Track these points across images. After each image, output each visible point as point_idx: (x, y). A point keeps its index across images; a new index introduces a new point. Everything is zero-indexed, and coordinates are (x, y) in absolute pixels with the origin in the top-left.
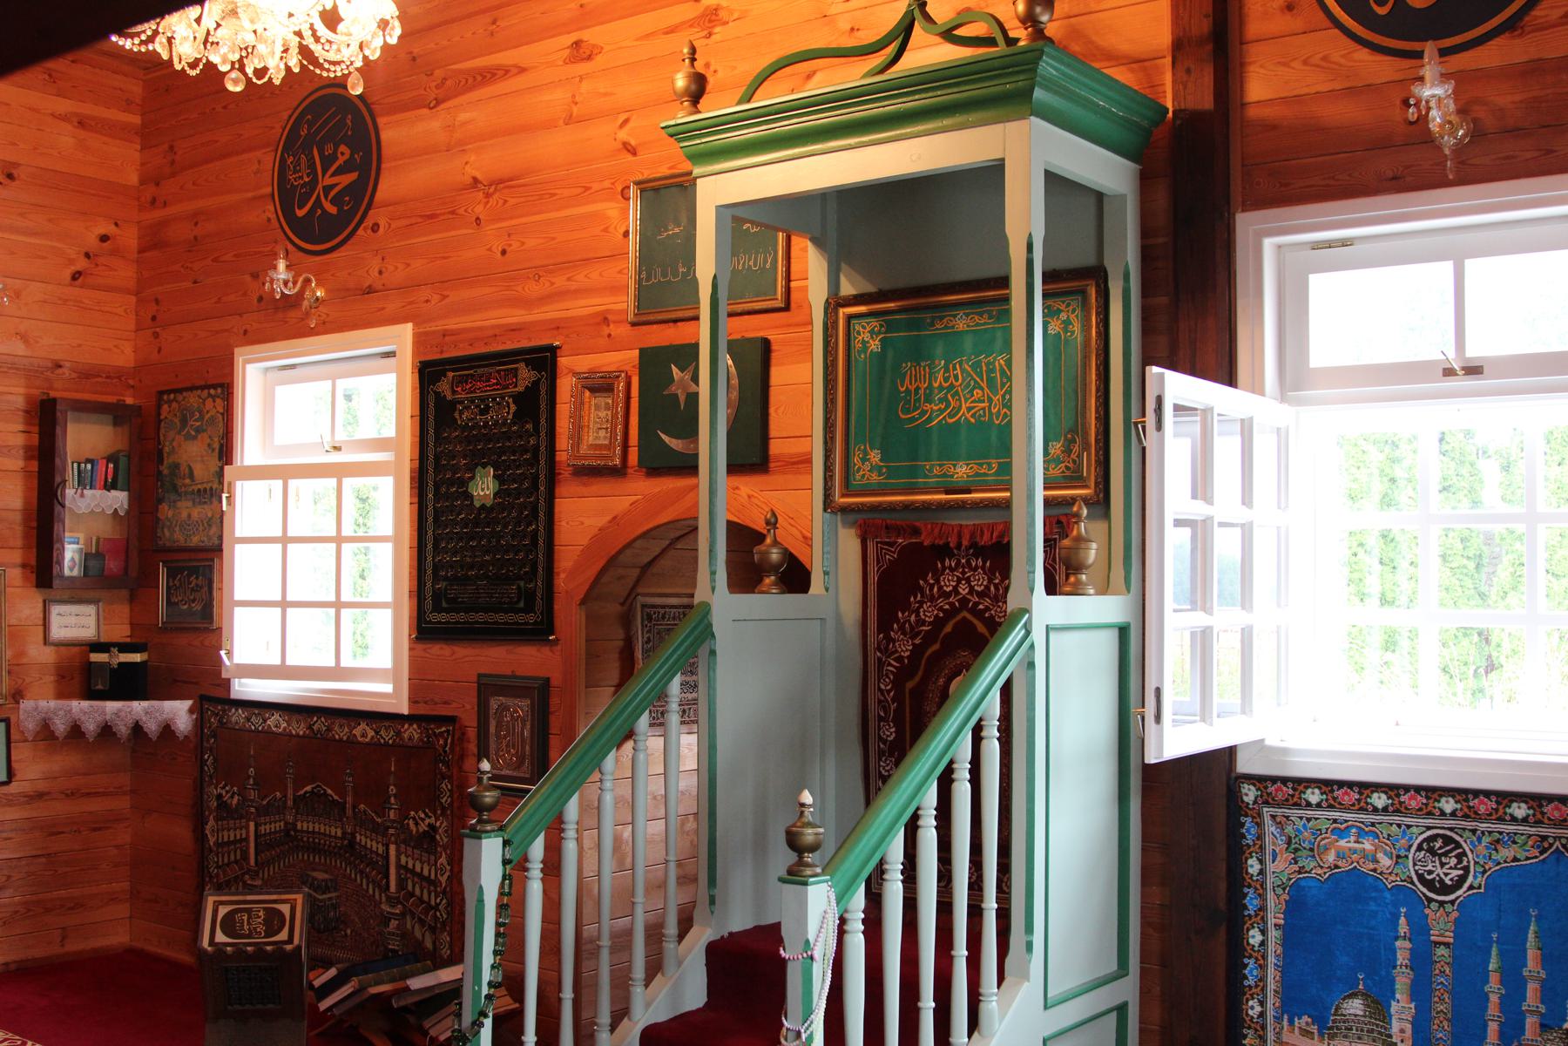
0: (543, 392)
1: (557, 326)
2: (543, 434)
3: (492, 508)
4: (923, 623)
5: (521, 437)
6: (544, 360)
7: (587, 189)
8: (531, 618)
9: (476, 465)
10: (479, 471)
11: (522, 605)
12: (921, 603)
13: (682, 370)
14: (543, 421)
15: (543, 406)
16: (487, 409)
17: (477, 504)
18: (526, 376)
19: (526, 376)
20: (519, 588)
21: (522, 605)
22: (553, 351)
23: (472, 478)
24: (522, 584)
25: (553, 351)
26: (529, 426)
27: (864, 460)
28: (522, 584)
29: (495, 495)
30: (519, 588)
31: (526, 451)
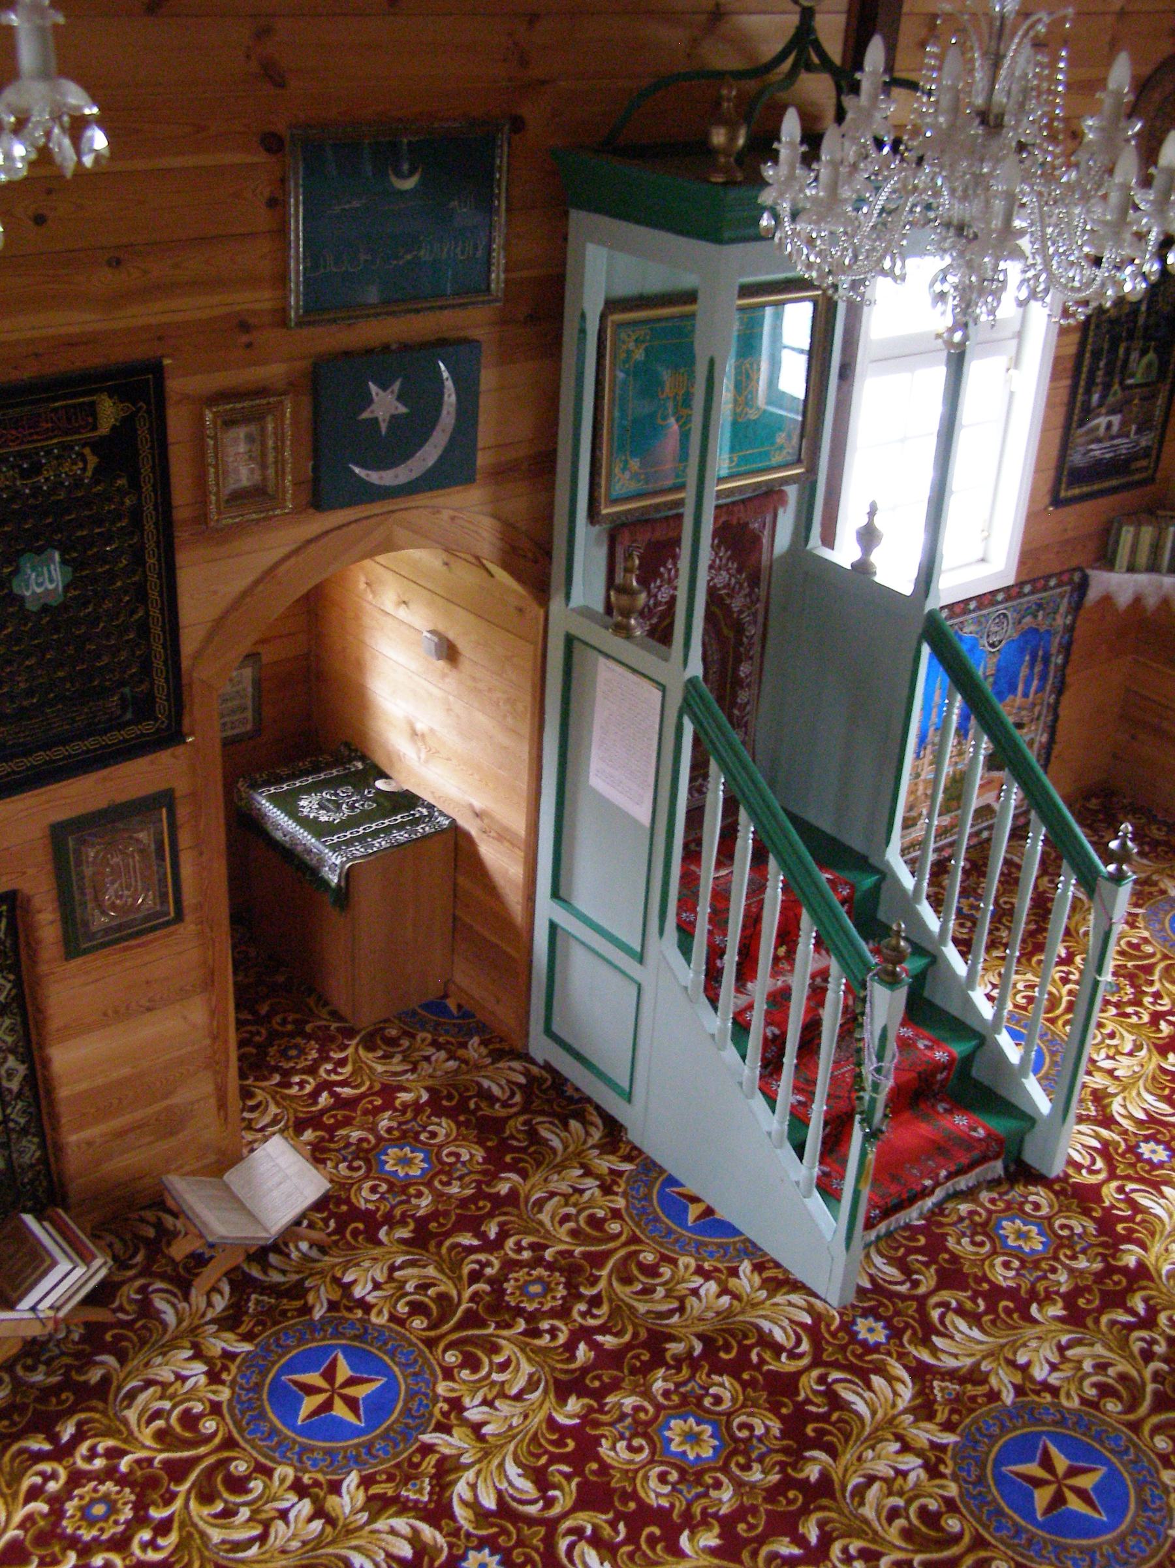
0: (143, 432)
2: (147, 489)
3: (64, 607)
4: (660, 603)
5: (110, 500)
6: (141, 383)
8: (148, 727)
9: (20, 553)
10: (27, 563)
12: (659, 587)
14: (146, 471)
16: (36, 469)
17: (32, 607)
18: (109, 412)
21: (129, 716)
22: (156, 369)
23: (16, 572)
27: (624, 469)
28: (127, 690)
29: (67, 588)
30: (123, 698)
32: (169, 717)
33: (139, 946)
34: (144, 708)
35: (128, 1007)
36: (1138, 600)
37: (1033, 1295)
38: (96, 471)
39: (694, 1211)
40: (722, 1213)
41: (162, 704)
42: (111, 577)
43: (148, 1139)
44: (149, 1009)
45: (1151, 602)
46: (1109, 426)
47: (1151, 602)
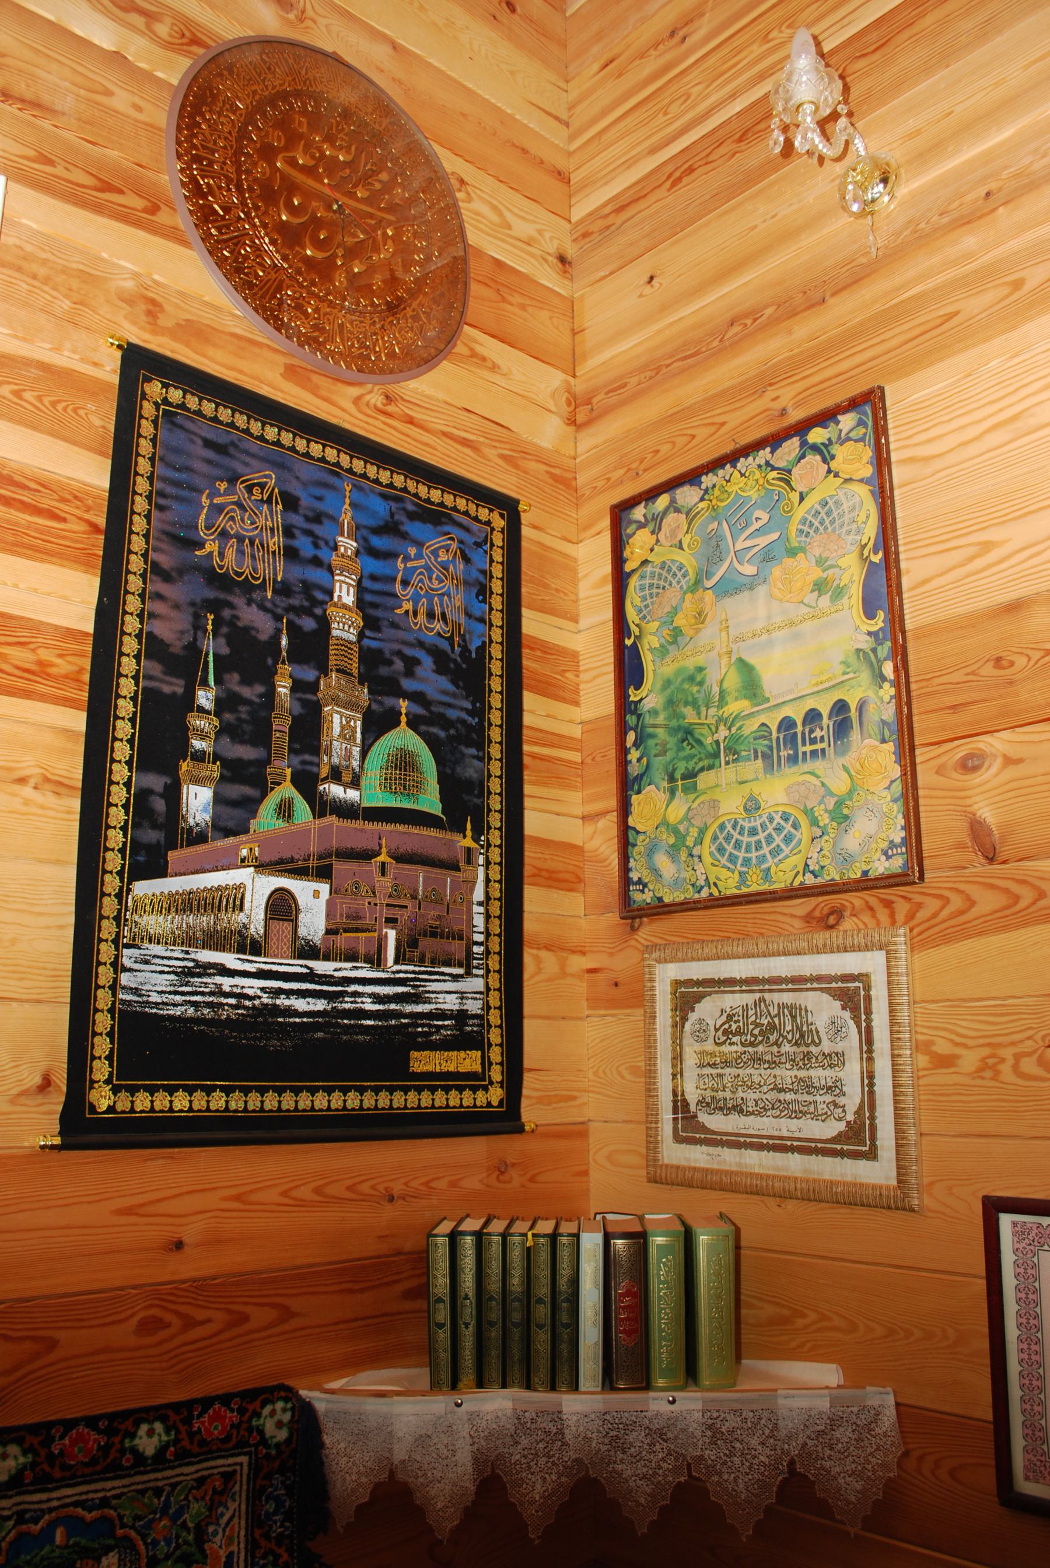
36: (492, 1481)
45: (537, 1486)
46: (282, 907)
47: (537, 1486)
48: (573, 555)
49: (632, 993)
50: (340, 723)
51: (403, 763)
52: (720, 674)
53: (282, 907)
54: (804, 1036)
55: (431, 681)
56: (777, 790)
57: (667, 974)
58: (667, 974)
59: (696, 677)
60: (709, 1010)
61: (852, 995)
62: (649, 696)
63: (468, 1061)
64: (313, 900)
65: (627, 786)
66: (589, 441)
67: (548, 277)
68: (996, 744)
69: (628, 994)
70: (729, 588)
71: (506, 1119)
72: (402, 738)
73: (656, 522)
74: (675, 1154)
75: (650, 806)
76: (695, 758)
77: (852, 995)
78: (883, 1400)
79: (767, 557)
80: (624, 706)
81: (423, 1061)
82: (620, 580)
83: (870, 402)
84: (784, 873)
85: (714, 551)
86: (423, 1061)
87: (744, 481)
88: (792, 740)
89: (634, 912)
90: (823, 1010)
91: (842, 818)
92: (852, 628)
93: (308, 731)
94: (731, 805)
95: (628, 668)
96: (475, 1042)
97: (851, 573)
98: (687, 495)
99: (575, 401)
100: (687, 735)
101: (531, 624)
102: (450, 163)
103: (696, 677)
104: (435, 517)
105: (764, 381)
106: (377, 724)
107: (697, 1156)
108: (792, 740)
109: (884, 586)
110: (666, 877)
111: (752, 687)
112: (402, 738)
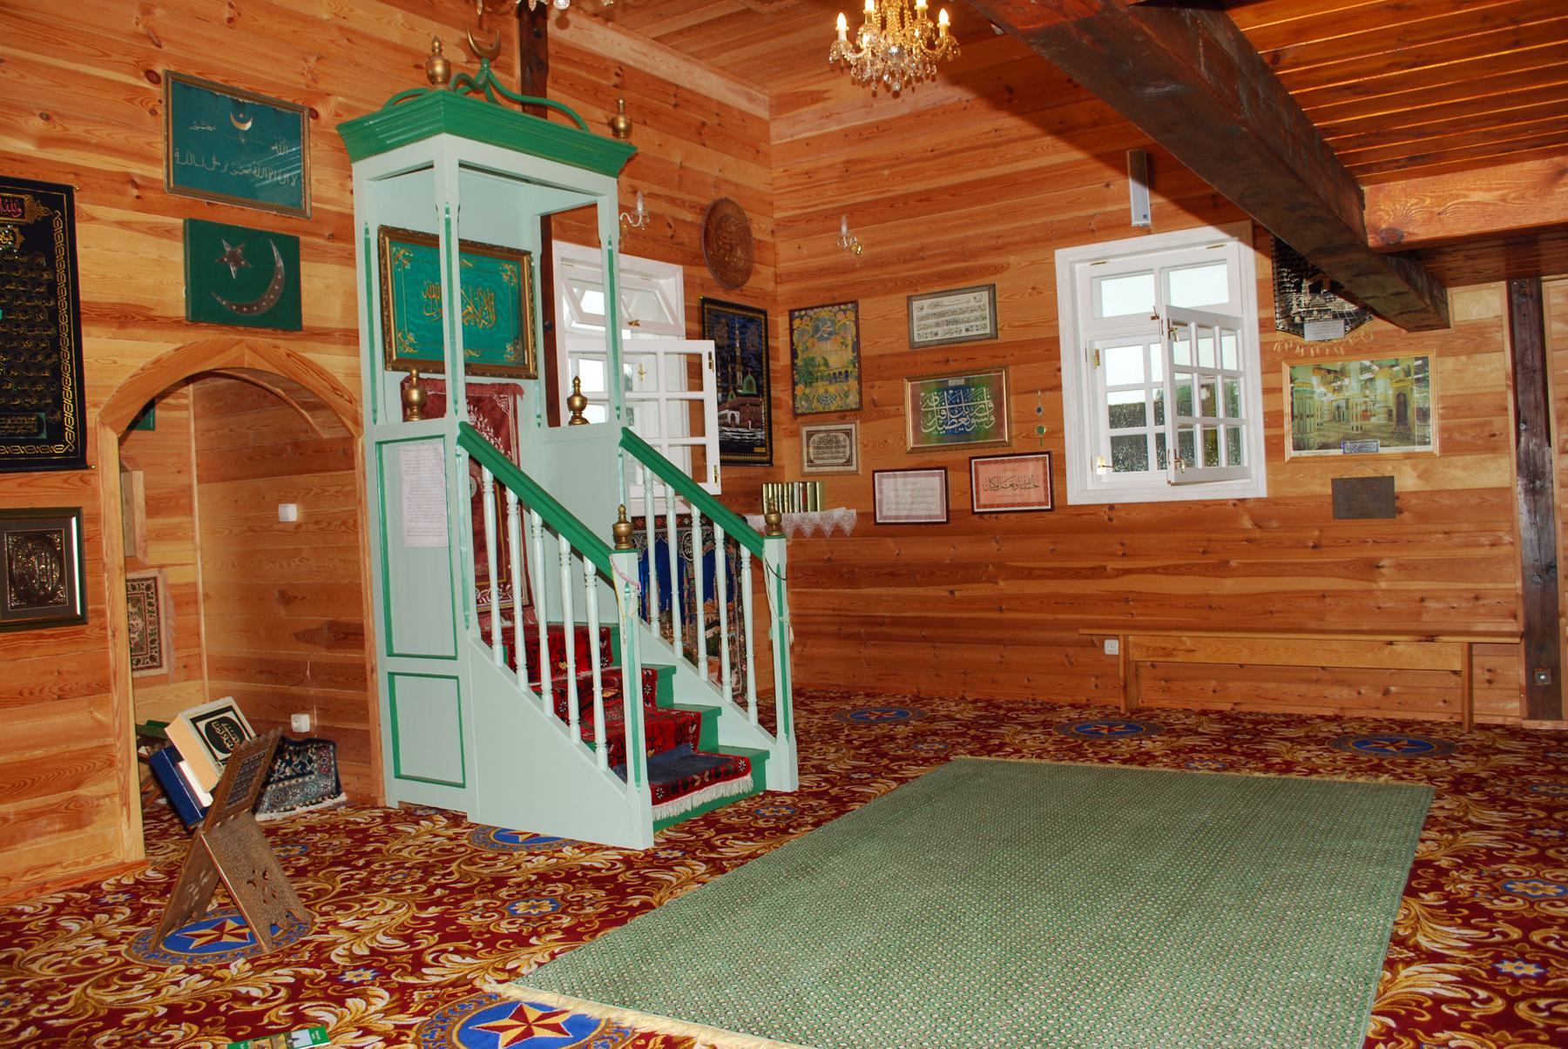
1: (77, 171)
7: (106, 55)
8: (59, 449)
11: (44, 436)
13: (233, 245)
14: (60, 256)
15: (59, 243)
18: (35, 210)
19: (35, 210)
20: (39, 419)
21: (44, 436)
24: (43, 415)
25: (69, 190)
26: (43, 261)
28: (43, 415)
31: (40, 285)
32: (75, 444)
33: (51, 636)
34: (57, 433)
35: (41, 691)
37: (788, 826)
38: (22, 245)
39: (521, 838)
40: (544, 832)
41: (69, 433)
42: (32, 327)
43: (57, 827)
44: (60, 698)
46: (733, 417)
48: (781, 322)
49: (797, 434)
50: (739, 375)
51: (750, 383)
52: (819, 360)
53: (733, 417)
54: (838, 442)
55: (754, 363)
56: (832, 389)
57: (805, 430)
58: (805, 430)
59: (813, 359)
60: (815, 438)
61: (848, 433)
62: (799, 362)
63: (763, 450)
64: (737, 414)
65: (794, 384)
66: (781, 289)
67: (769, 239)
68: (877, 383)
69: (796, 434)
70: (822, 339)
71: (770, 462)
72: (750, 377)
73: (801, 318)
74: (807, 469)
75: (800, 388)
76: (811, 379)
77: (848, 433)
78: (854, 512)
79: (830, 334)
80: (793, 364)
81: (757, 450)
82: (792, 331)
83: (855, 303)
84: (833, 407)
85: (817, 330)
86: (757, 450)
87: (825, 313)
88: (835, 378)
89: (796, 415)
90: (842, 437)
91: (847, 396)
92: (849, 355)
93: (734, 376)
94: (821, 391)
95: (794, 354)
96: (763, 445)
97: (850, 342)
98: (811, 313)
99: (776, 275)
100: (810, 373)
101: (771, 343)
102: (748, 215)
103: (813, 359)
104: (751, 320)
105: (829, 289)
106: (745, 374)
107: (814, 469)
108: (835, 378)
109: (857, 346)
110: (802, 405)
111: (826, 364)
112: (750, 377)
